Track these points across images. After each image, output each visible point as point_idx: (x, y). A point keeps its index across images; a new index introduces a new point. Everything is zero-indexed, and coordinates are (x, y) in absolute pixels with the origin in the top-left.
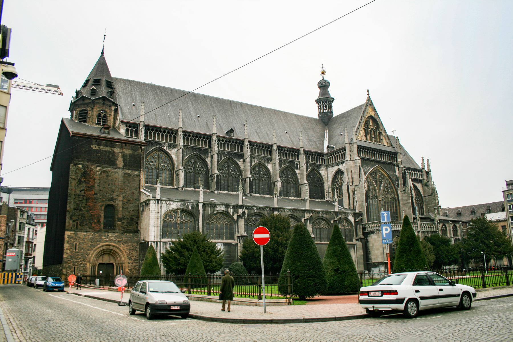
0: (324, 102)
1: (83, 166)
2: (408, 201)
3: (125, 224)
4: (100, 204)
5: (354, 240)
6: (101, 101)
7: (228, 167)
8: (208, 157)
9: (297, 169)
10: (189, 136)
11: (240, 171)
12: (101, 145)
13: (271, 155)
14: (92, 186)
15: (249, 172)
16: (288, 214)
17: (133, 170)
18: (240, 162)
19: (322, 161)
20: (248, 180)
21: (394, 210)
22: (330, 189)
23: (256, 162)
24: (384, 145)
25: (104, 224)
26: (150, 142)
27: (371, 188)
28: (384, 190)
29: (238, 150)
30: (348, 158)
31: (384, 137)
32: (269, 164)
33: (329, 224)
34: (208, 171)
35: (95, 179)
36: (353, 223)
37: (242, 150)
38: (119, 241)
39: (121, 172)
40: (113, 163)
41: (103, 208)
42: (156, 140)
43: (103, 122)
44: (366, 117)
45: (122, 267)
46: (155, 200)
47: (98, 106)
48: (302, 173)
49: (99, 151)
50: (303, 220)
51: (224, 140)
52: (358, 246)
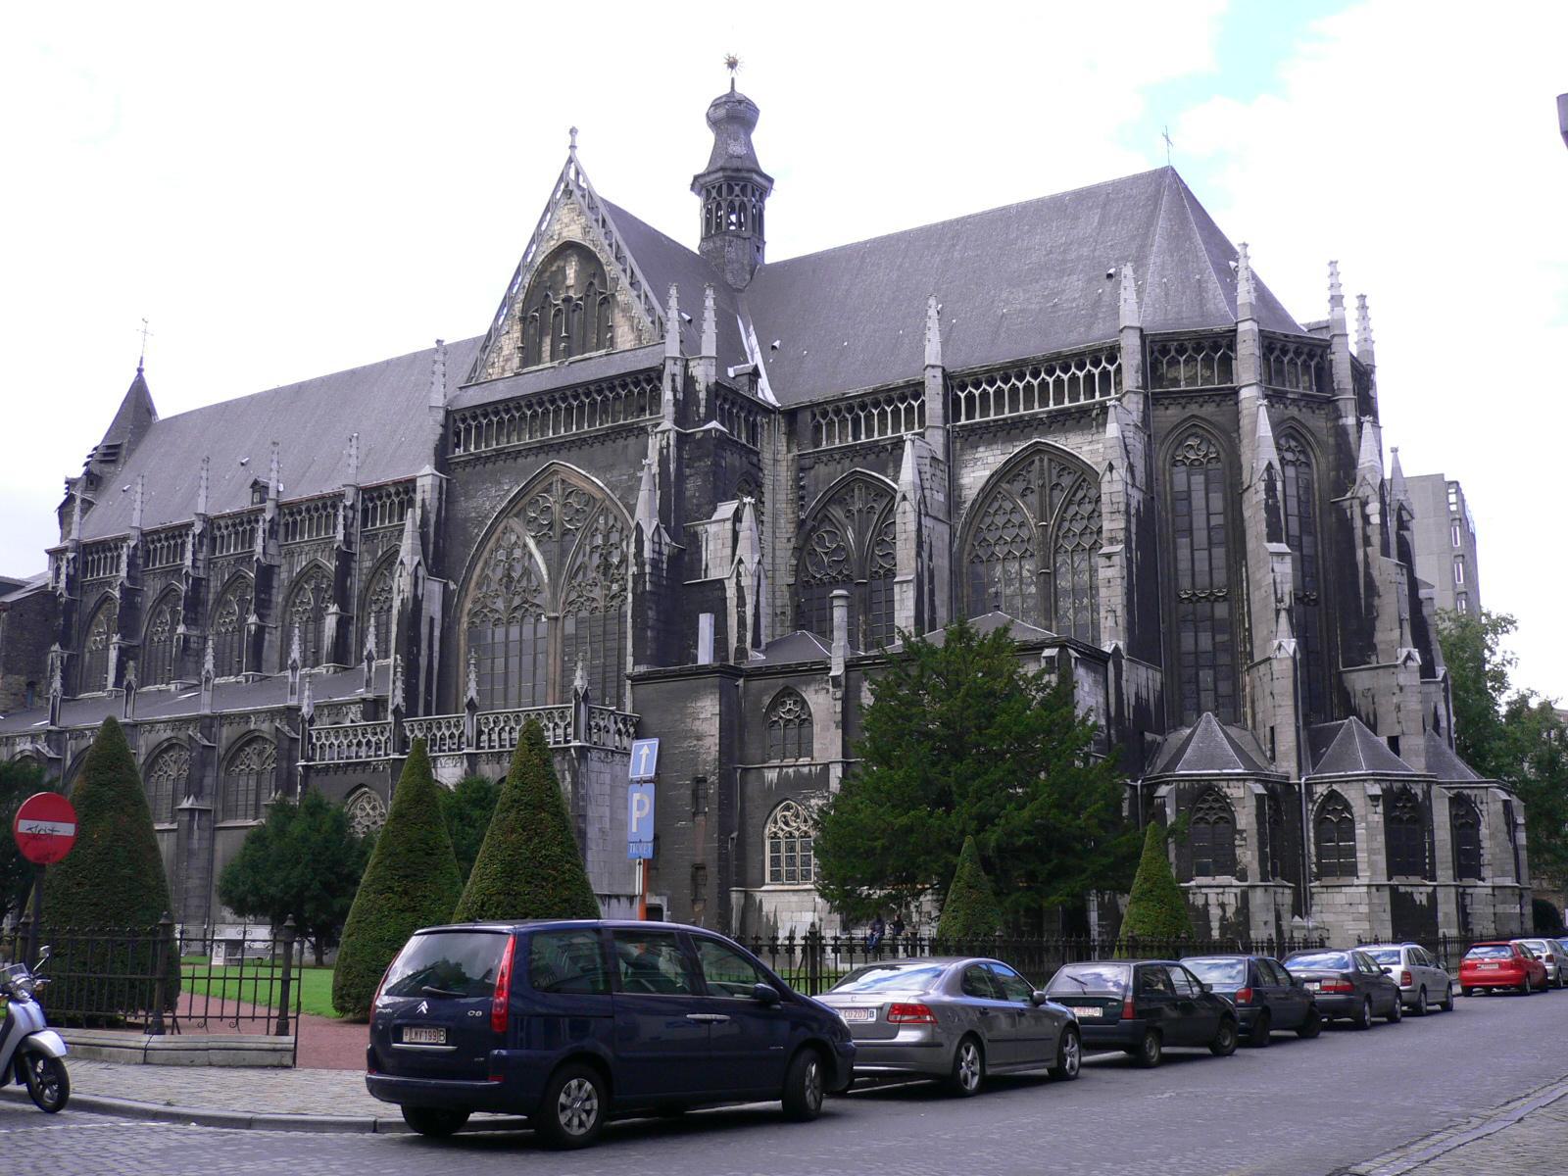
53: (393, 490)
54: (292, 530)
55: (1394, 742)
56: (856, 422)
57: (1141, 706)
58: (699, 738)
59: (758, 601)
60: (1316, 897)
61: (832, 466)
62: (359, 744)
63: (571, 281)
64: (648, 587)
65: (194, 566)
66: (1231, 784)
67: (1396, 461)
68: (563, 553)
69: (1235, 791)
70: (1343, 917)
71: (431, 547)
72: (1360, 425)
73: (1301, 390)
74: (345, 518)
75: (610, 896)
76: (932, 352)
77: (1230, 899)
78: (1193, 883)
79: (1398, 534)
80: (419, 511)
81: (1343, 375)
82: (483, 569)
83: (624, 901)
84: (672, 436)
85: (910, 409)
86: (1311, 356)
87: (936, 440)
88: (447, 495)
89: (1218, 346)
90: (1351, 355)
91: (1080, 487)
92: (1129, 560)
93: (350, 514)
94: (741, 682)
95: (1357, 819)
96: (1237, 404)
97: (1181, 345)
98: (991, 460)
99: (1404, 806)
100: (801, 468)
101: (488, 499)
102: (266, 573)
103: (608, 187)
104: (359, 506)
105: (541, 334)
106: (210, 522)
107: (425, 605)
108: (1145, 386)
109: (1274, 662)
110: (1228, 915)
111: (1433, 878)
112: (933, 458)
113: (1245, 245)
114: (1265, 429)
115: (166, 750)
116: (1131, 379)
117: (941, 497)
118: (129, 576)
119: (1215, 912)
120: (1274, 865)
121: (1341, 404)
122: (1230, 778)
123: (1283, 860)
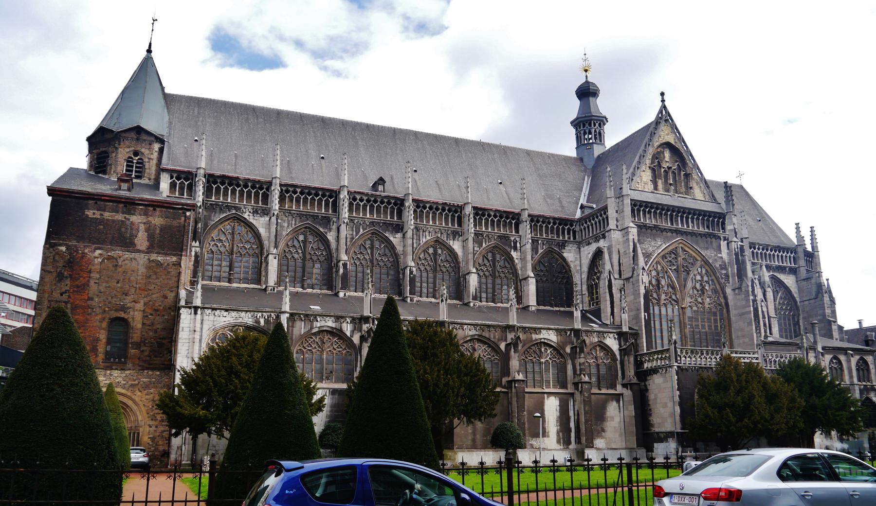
0: (587, 125)
1: (67, 249)
2: (747, 310)
3: (146, 353)
4: (99, 317)
5: (619, 387)
6: (133, 135)
7: (372, 247)
8: (330, 230)
9: (515, 249)
10: (295, 192)
11: (396, 255)
12: (104, 211)
13: (460, 225)
14: (84, 285)
15: (410, 258)
16: (471, 333)
17: (166, 254)
18: (395, 239)
19: (569, 233)
20: (408, 271)
21: (716, 327)
22: (585, 287)
23: (428, 238)
24: (698, 200)
25: (107, 353)
26: (217, 205)
27: (663, 282)
28: (694, 288)
29: (392, 217)
30: (612, 224)
31: (697, 183)
32: (456, 242)
33: (561, 355)
34: (332, 257)
35: (90, 272)
36: (617, 353)
37: (400, 215)
38: (132, 385)
39: (142, 259)
40: (128, 244)
41: (104, 325)
42: (229, 200)
43: (136, 172)
44: (656, 144)
45: (138, 433)
46: (190, 308)
47: (127, 143)
48: (524, 257)
49: (101, 221)
50: (502, 346)
51: (365, 198)
52: (625, 399)
53: (492, 214)
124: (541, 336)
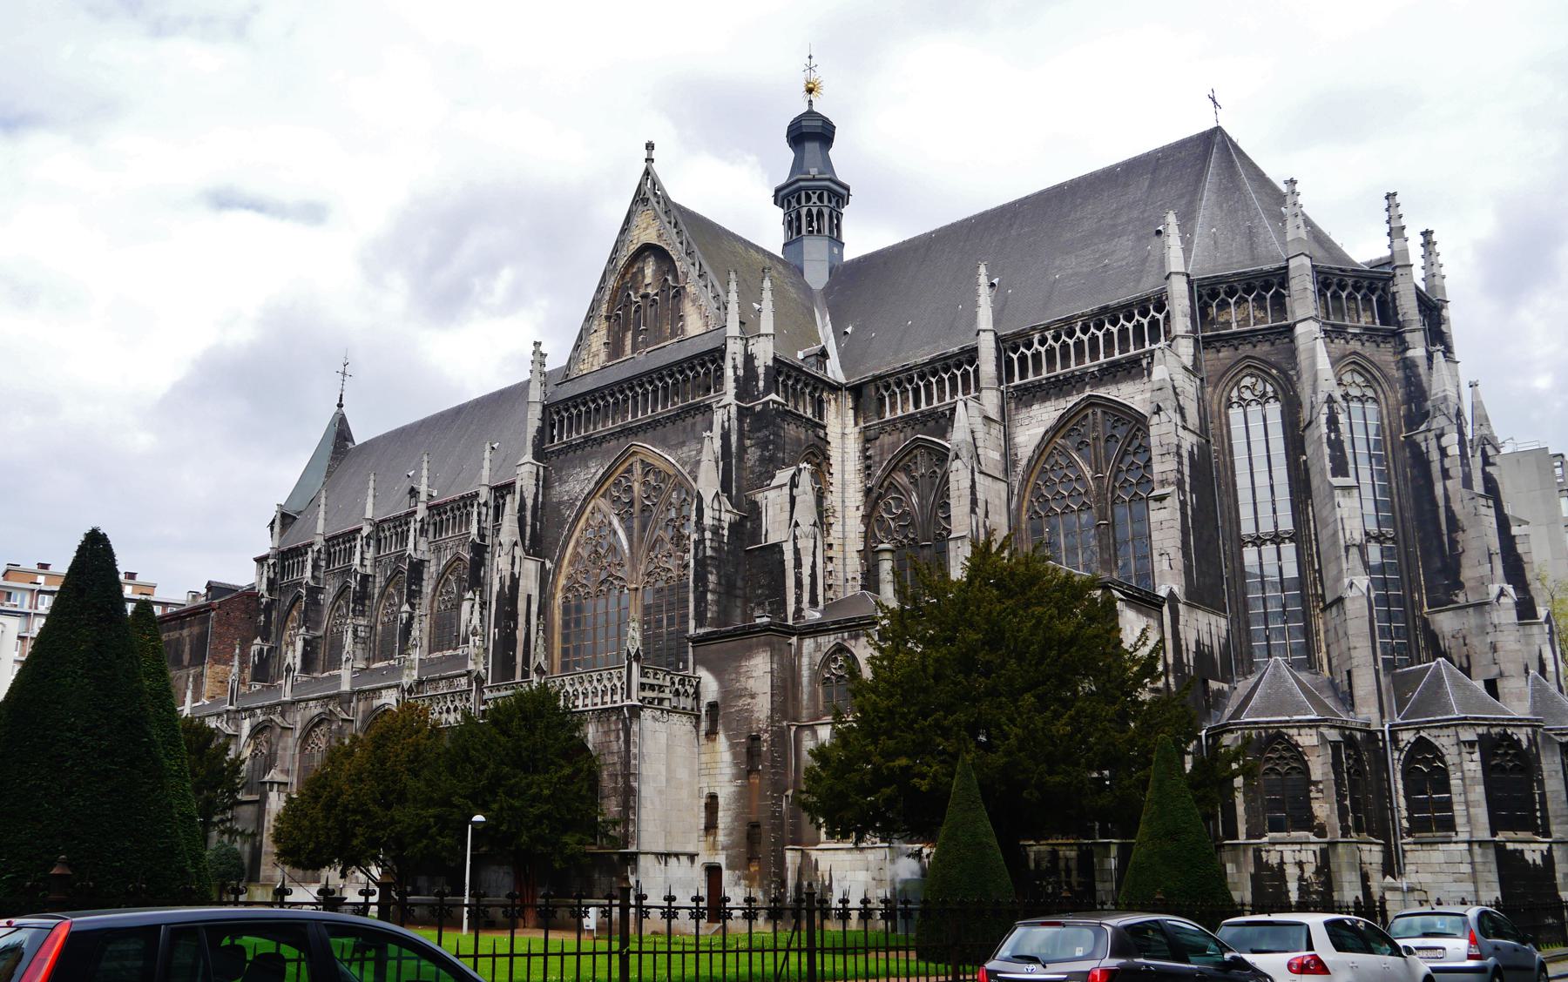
31: (694, 301)
54: (439, 528)
55: (1491, 686)
56: (917, 391)
57: (1202, 654)
58: (753, 696)
59: (814, 563)
60: (1408, 855)
61: (894, 438)
62: (448, 711)
63: (648, 281)
64: (709, 552)
65: (362, 565)
66: (1303, 731)
67: (1475, 395)
68: (644, 528)
69: (1307, 739)
70: (1442, 877)
71: (528, 529)
72: (1430, 357)
73: (1363, 323)
74: (479, 514)
75: (668, 855)
76: (985, 318)
77: (1309, 856)
78: (1265, 839)
79: (1483, 470)
80: (518, 497)
81: (1408, 308)
82: (575, 548)
83: (684, 859)
84: (733, 410)
85: (966, 375)
86: (1373, 291)
87: (991, 400)
88: (545, 483)
89: (1269, 286)
90: (1417, 288)
91: (1135, 436)
92: (1183, 504)
93: (484, 510)
94: (794, 640)
95: (1451, 768)
96: (1292, 341)
97: (1231, 287)
98: (1045, 417)
99: (1506, 754)
100: (867, 440)
101: (578, 482)
102: (417, 567)
103: (682, 190)
104: (492, 503)
105: (626, 330)
106: (378, 526)
107: (521, 582)
108: (1194, 331)
109: (1347, 603)
110: (1306, 875)
111: (1547, 834)
112: (986, 418)
113: (1293, 182)
114: (1324, 363)
115: (318, 725)
116: (1181, 324)
117: (996, 456)
118: (313, 577)
119: (1291, 871)
120: (1357, 820)
121: (1408, 336)
122: (1300, 725)
123: (1366, 813)
124: (382, 701)
